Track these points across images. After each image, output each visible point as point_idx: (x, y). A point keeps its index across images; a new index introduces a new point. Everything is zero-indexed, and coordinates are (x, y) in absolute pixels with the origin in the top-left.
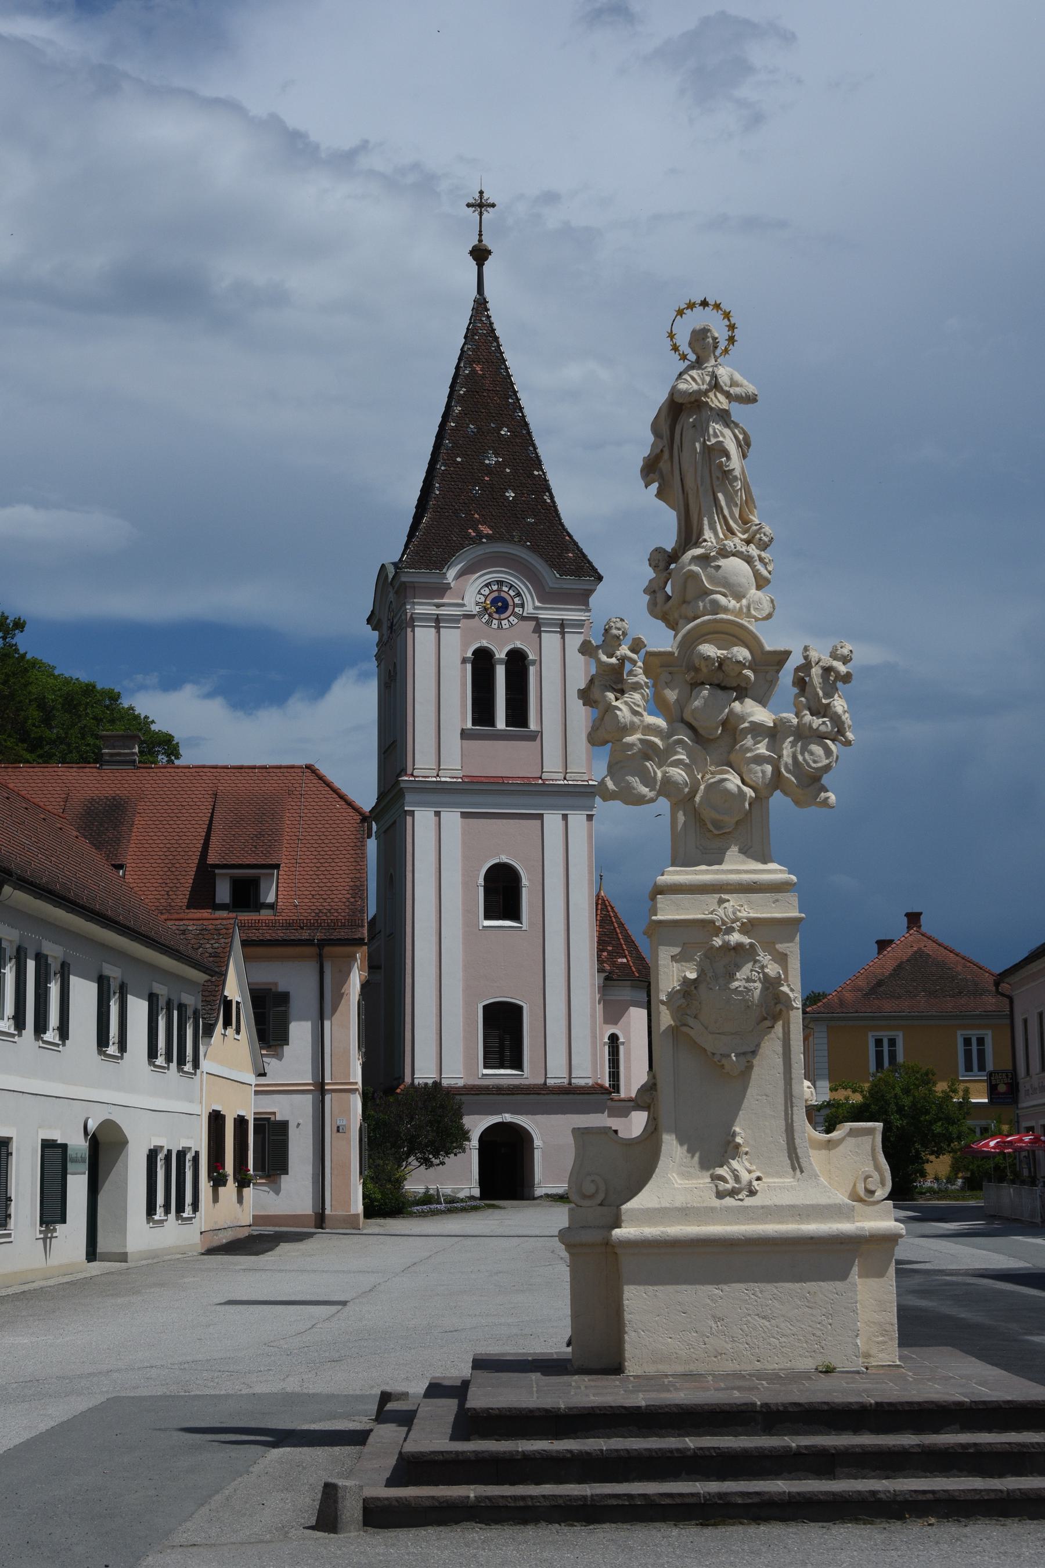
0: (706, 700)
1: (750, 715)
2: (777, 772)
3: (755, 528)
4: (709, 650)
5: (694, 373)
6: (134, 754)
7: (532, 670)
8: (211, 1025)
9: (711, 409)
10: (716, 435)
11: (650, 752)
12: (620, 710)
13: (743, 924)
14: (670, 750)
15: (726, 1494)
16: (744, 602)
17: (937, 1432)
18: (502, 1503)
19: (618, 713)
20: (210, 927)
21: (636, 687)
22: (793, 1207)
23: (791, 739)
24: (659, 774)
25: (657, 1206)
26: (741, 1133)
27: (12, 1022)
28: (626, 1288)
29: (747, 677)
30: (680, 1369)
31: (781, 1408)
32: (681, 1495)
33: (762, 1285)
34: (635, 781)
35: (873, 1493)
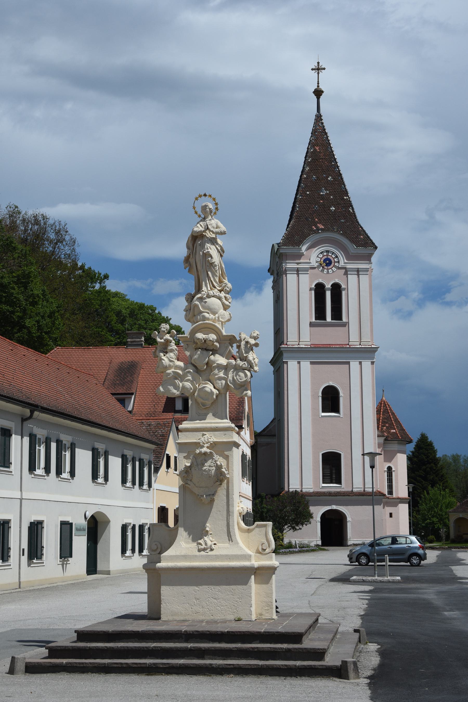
0: (199, 355)
1: (217, 361)
2: (226, 383)
3: (224, 285)
4: (200, 336)
5: (201, 223)
6: (142, 341)
7: (344, 293)
8: (158, 467)
9: (207, 237)
10: (208, 249)
12: (164, 360)
13: (211, 444)
14: (185, 375)
15: (157, 664)
16: (217, 315)
17: (250, 643)
18: (75, 665)
19: (163, 361)
20: (162, 423)
21: (172, 351)
22: (227, 555)
23: (232, 370)
24: (181, 385)
25: (175, 554)
26: (208, 526)
27: (44, 470)
28: (162, 587)
29: (216, 346)
30: (182, 618)
31: (191, 633)
32: (140, 663)
33: (214, 587)
34: (171, 388)
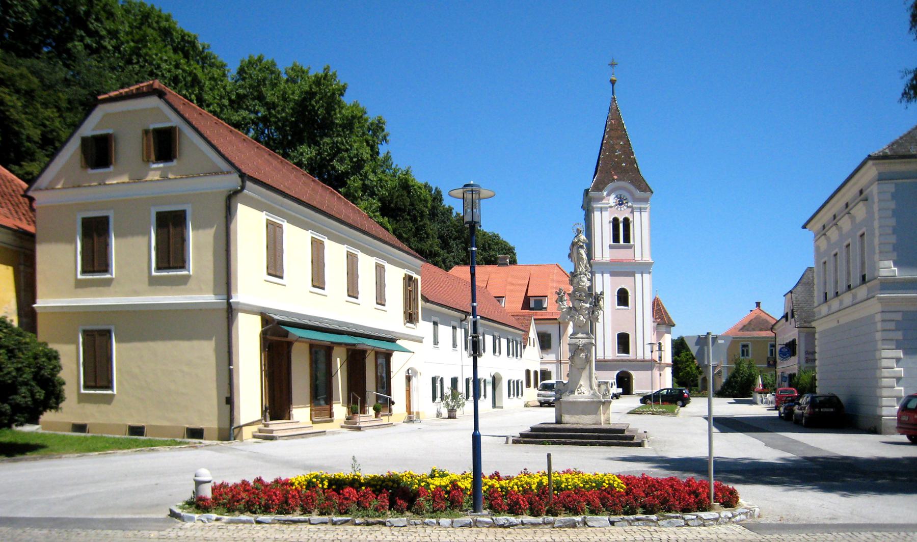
7: (631, 225)
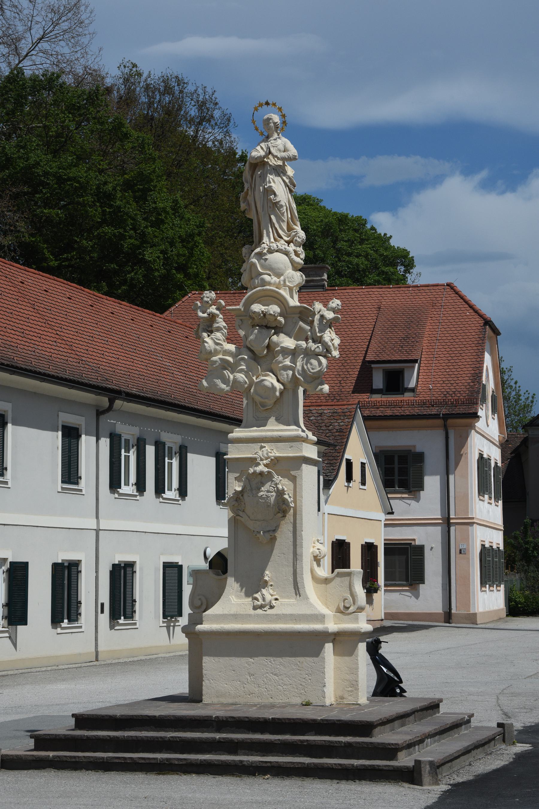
0: (256, 335)
1: (281, 343)
2: (294, 374)
3: (294, 234)
4: (257, 308)
5: (263, 145)
6: (324, 280)
8: (330, 480)
9: (270, 165)
10: (270, 182)
11: (226, 366)
12: (207, 343)
13: (272, 460)
14: (237, 363)
15: (170, 759)
16: (282, 278)
17: (303, 735)
18: (65, 759)
19: (206, 344)
20: (340, 411)
21: (219, 329)
22: (291, 615)
23: (302, 356)
24: (232, 377)
25: (222, 613)
26: (268, 575)
27: (135, 487)
28: (204, 658)
29: (280, 322)
30: (230, 701)
31: (225, 719)
32: (149, 759)
33: (274, 658)
34: (218, 382)
35: (241, 761)
